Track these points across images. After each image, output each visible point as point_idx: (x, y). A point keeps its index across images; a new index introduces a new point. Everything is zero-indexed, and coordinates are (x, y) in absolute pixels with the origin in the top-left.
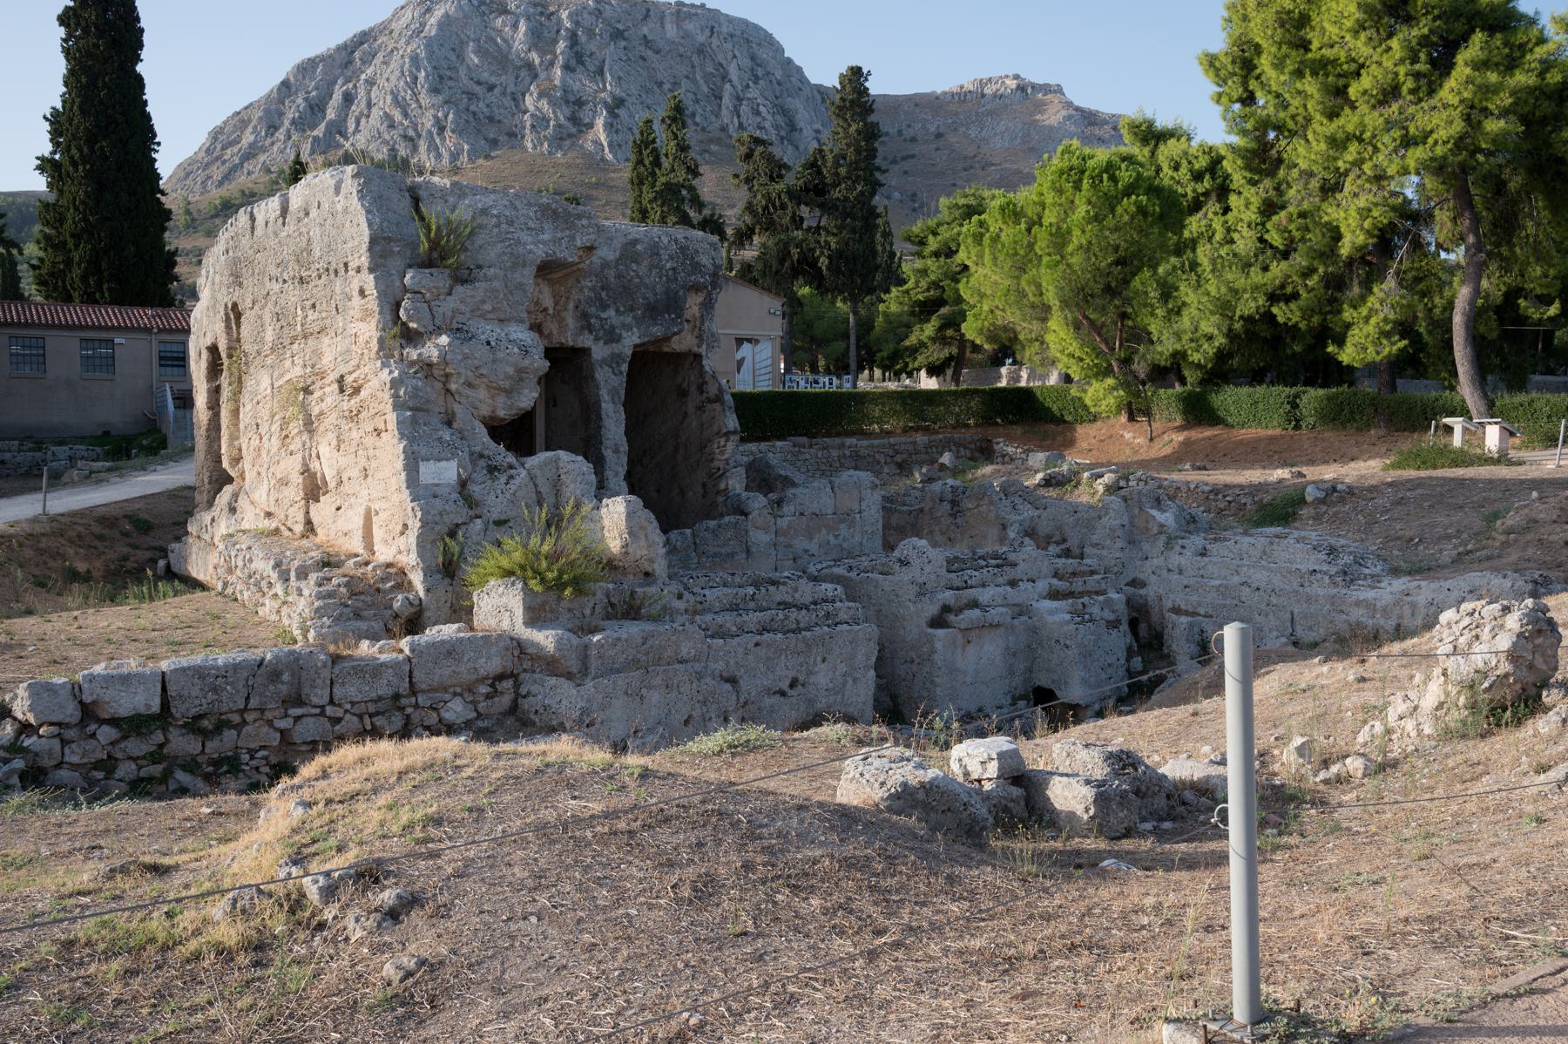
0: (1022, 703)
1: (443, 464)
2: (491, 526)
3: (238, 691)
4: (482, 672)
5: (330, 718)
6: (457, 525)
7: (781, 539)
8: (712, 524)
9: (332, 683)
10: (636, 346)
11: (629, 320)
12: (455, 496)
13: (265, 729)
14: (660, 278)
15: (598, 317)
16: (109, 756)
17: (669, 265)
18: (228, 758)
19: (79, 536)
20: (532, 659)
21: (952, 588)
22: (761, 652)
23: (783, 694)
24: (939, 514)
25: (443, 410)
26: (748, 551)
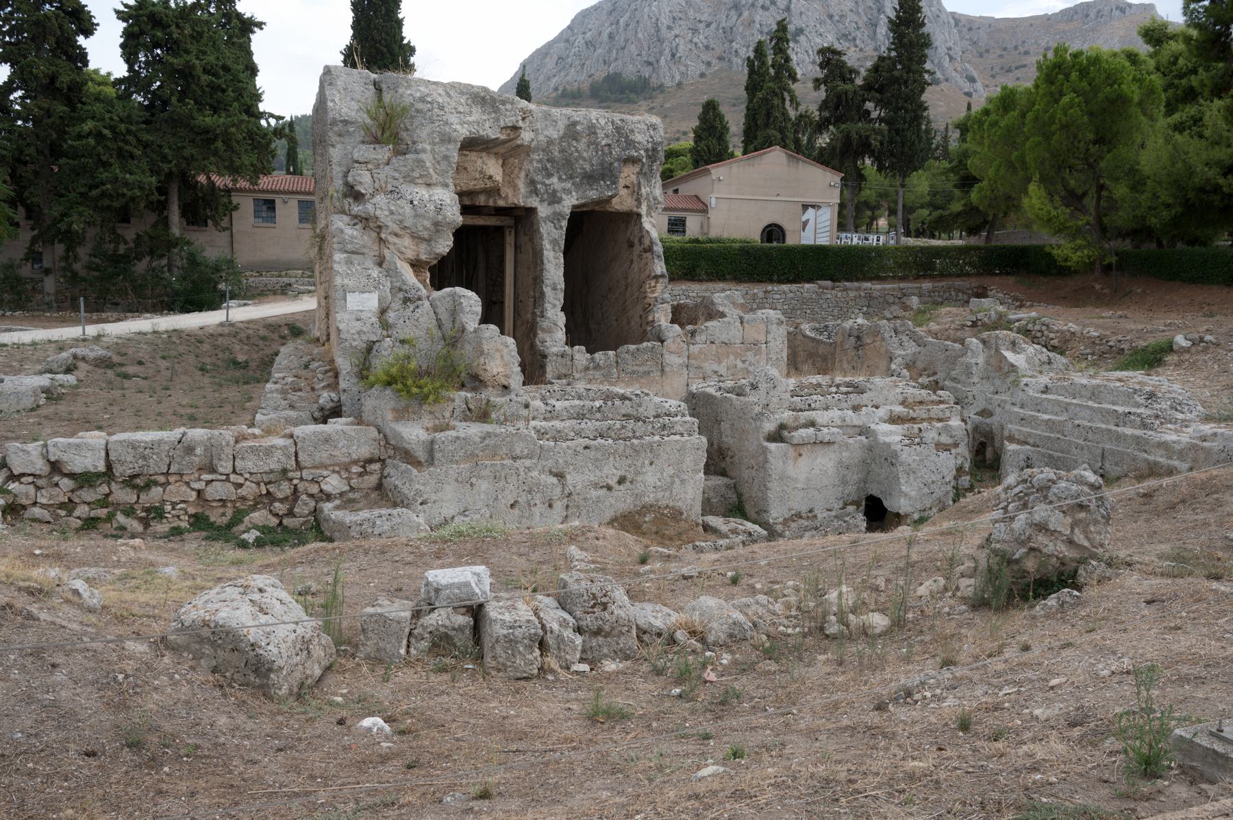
0: (851, 508)
1: (366, 295)
2: (398, 344)
3: (162, 459)
4: (354, 456)
5: (233, 483)
6: (374, 342)
7: (693, 362)
8: (632, 347)
9: (234, 458)
10: (574, 207)
11: (568, 185)
12: (374, 320)
13: (184, 488)
14: (597, 152)
15: (543, 184)
16: (70, 500)
17: (603, 143)
18: (156, 507)
19: (248, 338)
20: (394, 449)
21: (793, 410)
22: (591, 454)
23: (609, 488)
24: (847, 347)
25: (377, 254)
26: (663, 370)
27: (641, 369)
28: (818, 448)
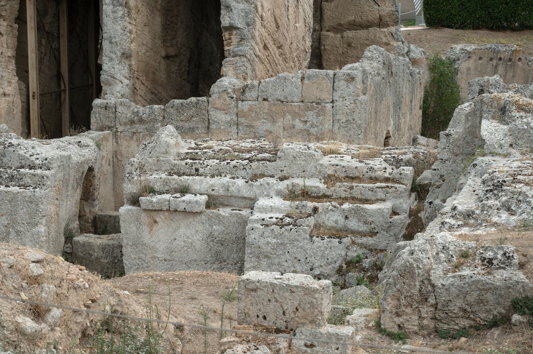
7: (242, 120)
26: (208, 128)
27: (187, 125)
28: (180, 216)
